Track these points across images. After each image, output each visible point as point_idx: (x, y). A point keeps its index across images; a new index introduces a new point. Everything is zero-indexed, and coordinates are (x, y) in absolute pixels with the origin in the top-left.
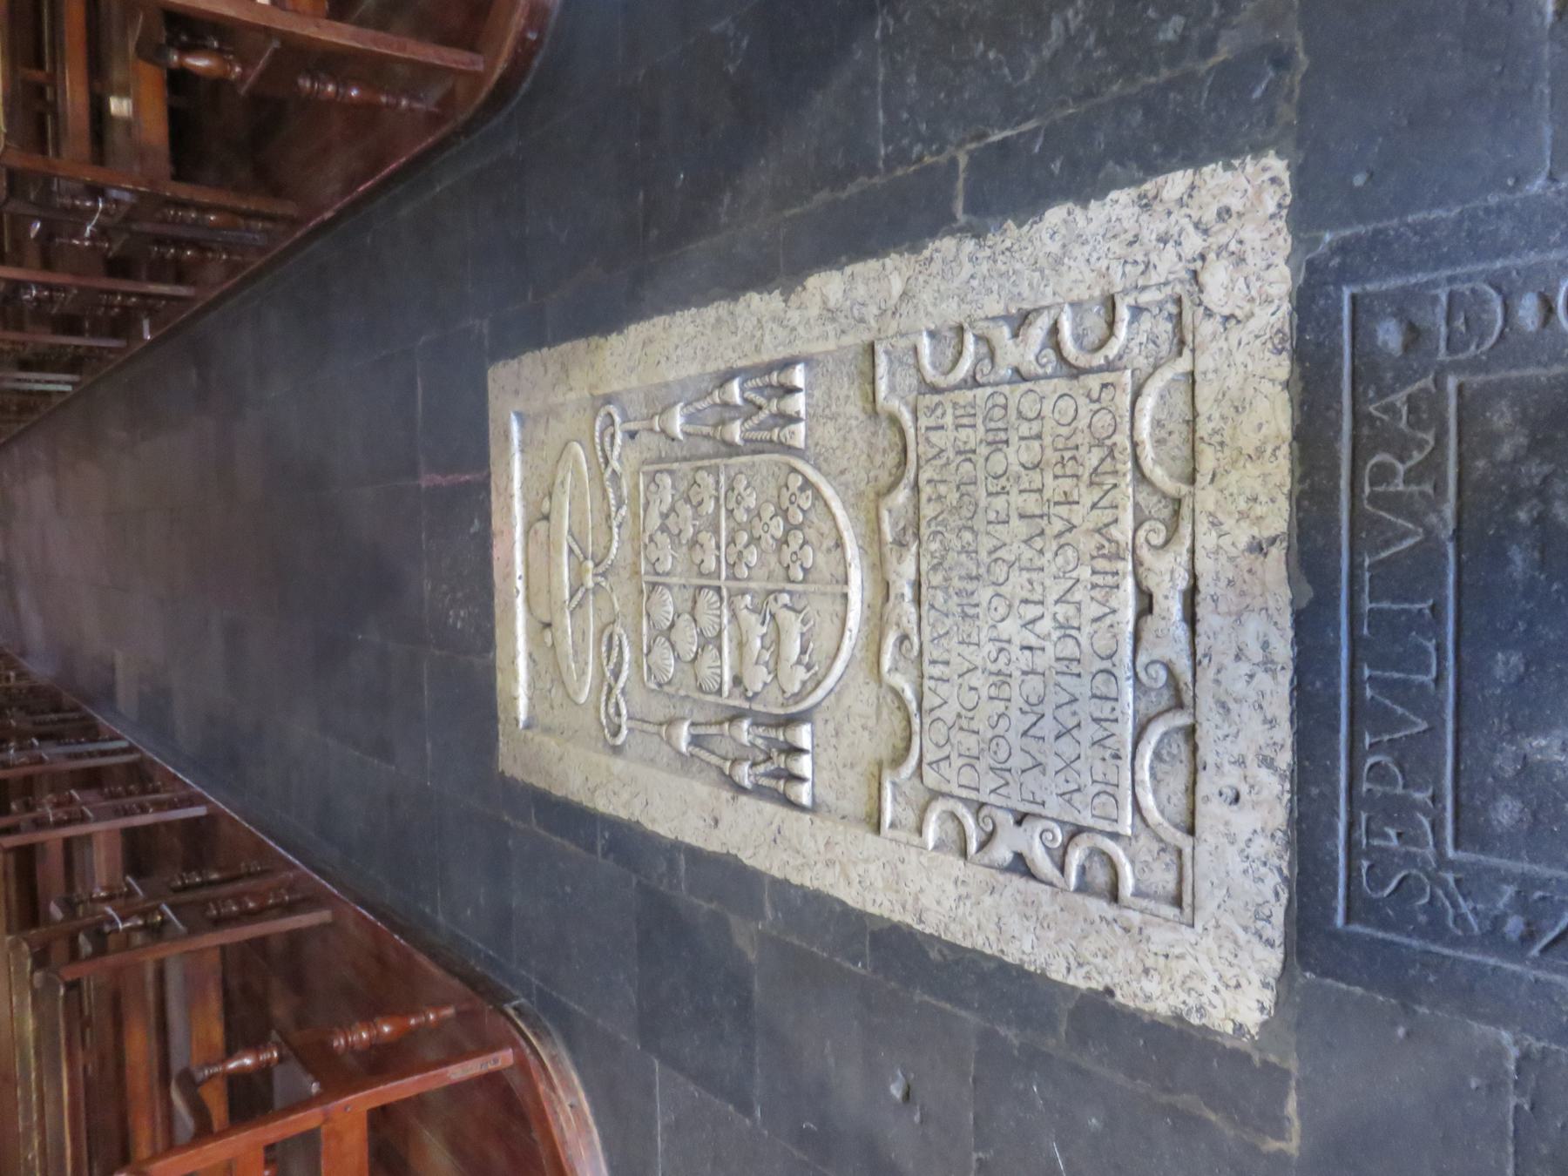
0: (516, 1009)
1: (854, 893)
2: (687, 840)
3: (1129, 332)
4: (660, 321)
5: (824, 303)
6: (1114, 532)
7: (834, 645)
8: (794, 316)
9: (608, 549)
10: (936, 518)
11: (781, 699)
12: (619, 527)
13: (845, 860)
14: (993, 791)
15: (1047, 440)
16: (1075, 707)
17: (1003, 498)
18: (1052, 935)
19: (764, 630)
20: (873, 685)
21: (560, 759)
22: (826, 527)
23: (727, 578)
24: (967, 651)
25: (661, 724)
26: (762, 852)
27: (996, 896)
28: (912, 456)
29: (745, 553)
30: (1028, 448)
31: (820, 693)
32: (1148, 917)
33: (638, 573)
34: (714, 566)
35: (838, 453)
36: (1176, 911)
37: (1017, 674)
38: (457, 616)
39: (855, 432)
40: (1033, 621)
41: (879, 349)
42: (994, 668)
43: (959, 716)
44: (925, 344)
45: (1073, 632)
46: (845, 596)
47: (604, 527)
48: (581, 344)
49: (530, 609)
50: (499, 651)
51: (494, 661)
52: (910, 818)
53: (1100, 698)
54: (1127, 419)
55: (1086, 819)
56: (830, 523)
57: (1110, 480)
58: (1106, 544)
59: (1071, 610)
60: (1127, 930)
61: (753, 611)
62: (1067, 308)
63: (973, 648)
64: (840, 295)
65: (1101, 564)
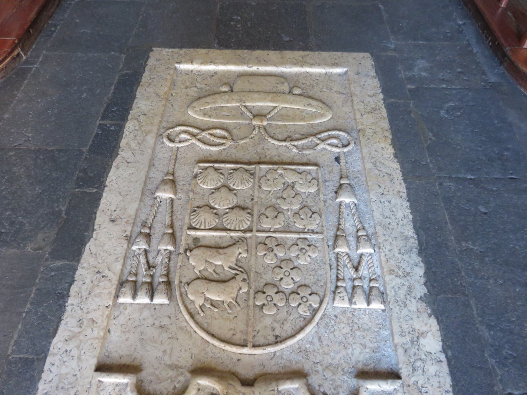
0: (18, 55)
1: (60, 345)
2: (104, 195)
4: (403, 188)
5: (422, 333)
7: (215, 330)
8: (414, 305)
9: (272, 138)
11: (184, 280)
12: (286, 146)
13: (81, 337)
19: (226, 268)
21: (157, 95)
22: (288, 328)
23: (257, 237)
25: (173, 174)
26: (92, 261)
29: (272, 254)
31: (187, 317)
33: (259, 163)
34: (266, 226)
35: (332, 336)
38: (238, 22)
39: (344, 352)
46: (244, 345)
47: (285, 135)
48: (385, 124)
49: (241, 75)
50: (218, 52)
51: (213, 48)
56: (290, 332)
61: (237, 260)
64: (428, 349)
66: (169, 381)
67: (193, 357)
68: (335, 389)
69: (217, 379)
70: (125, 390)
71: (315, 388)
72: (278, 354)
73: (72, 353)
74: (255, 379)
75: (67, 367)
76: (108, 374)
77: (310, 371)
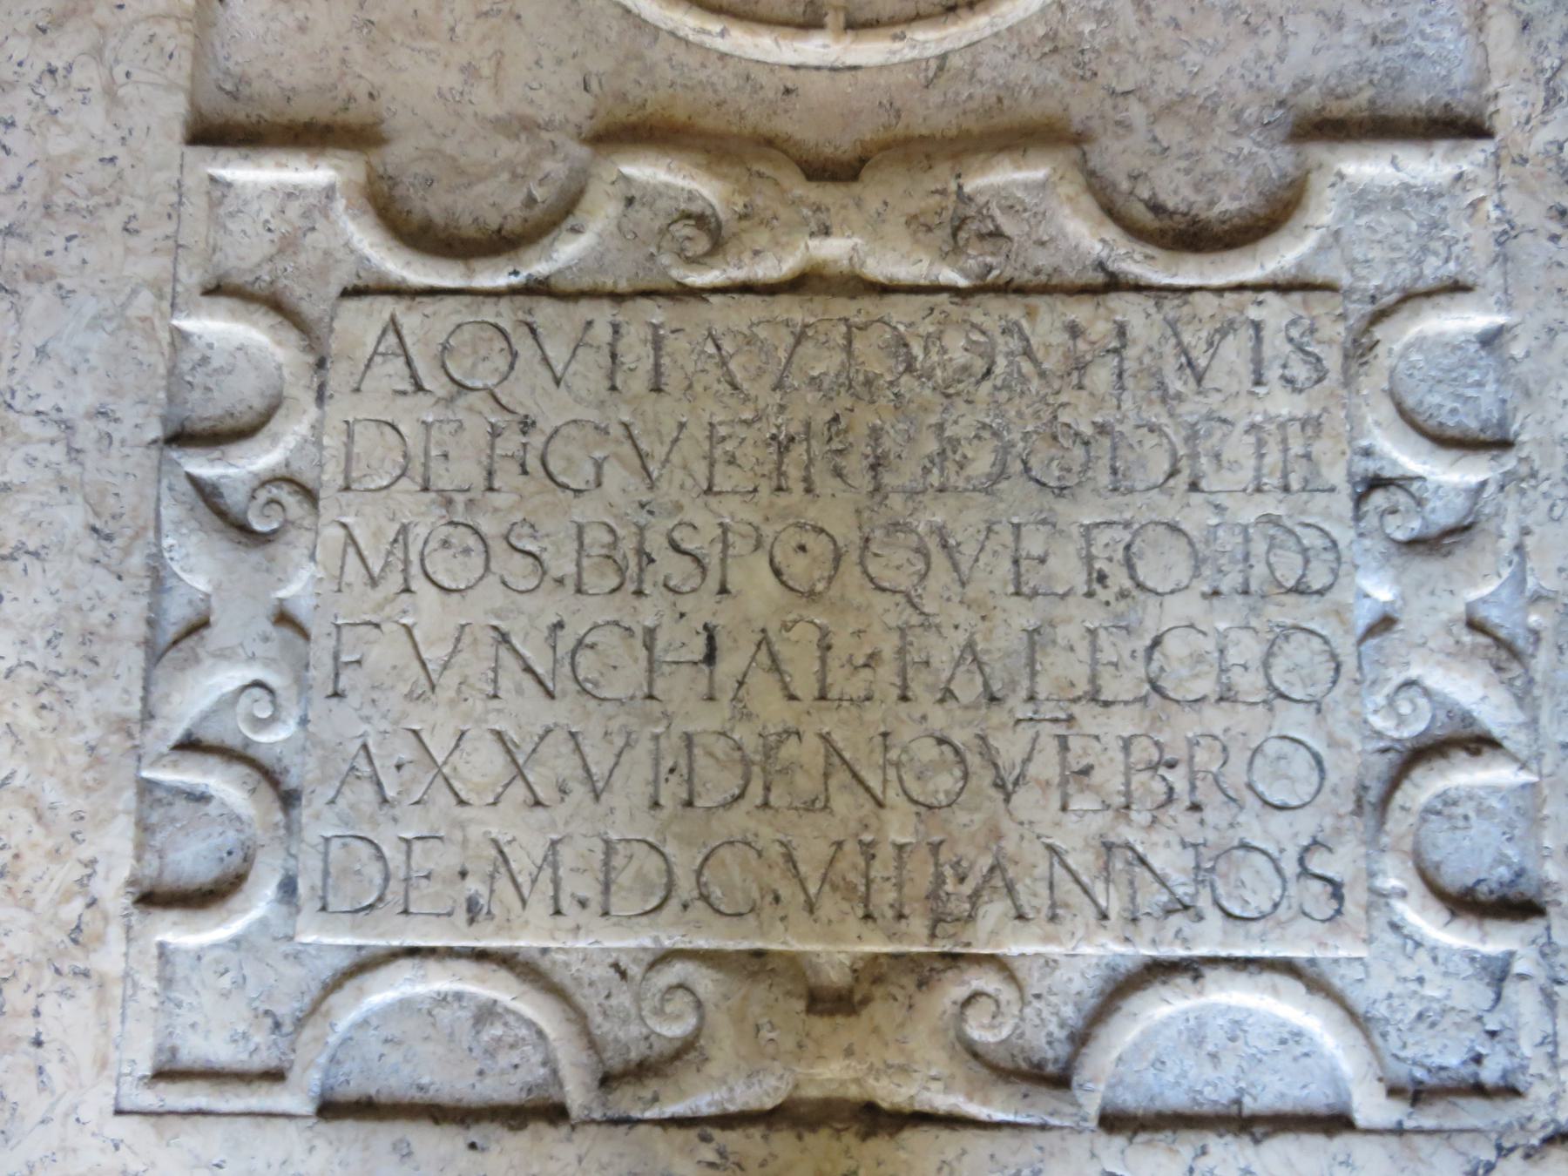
3: (1451, 951)
6: (994, 911)
10: (1028, 353)
14: (351, 539)
15: (1216, 719)
16: (579, 792)
17: (1080, 582)
18: (26, 718)
20: (582, 109)
24: (692, 449)
27: (89, 546)
28: (1189, 271)
30: (1198, 658)
32: (117, 991)
36: (146, 1068)
37: (647, 613)
40: (775, 666)
41: (1473, 157)
42: (656, 543)
43: (527, 425)
44: (1462, 320)
45: (756, 789)
46: (810, 24)
52: (245, 253)
53: (606, 863)
54: (1256, 952)
55: (317, 820)
57: (1114, 904)
58: (967, 888)
59: (807, 784)
60: (76, 934)
62: (1525, 777)
63: (701, 469)
65: (921, 875)
66: (505, 176)
67: (594, 85)
68: (1197, 188)
69: (701, 158)
70: (325, 212)
71: (1114, 185)
72: (955, 62)
73: (78, 77)
74: (862, 161)
75: (68, 131)
76: (244, 151)
77: (1096, 123)
